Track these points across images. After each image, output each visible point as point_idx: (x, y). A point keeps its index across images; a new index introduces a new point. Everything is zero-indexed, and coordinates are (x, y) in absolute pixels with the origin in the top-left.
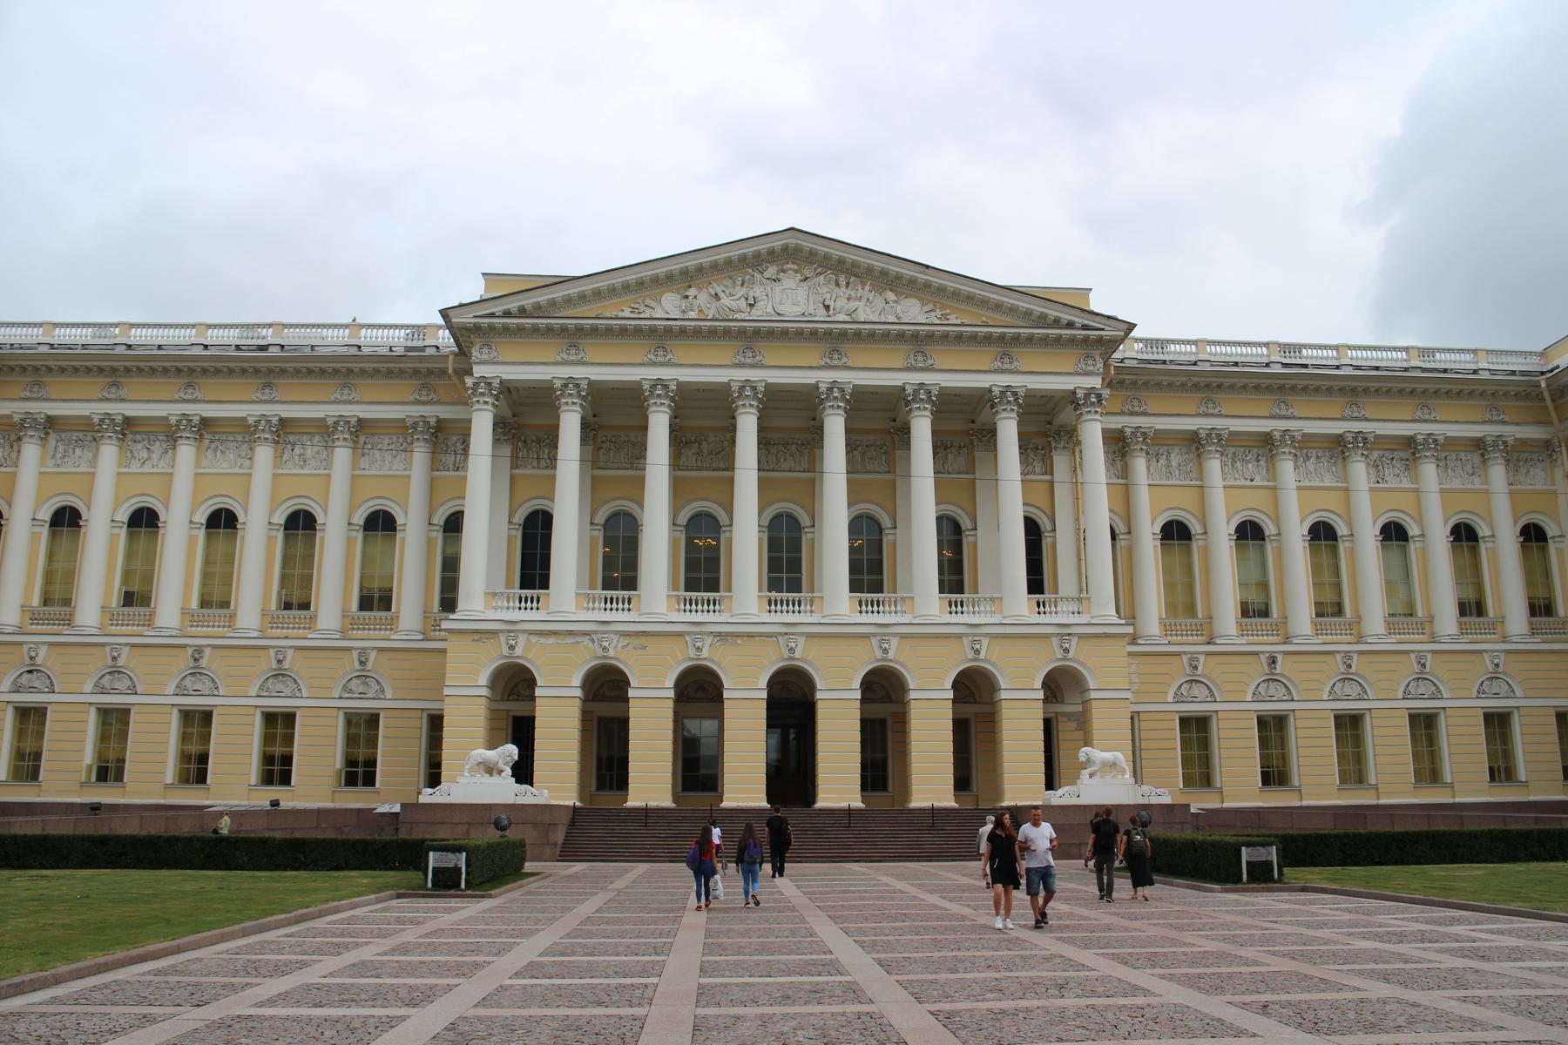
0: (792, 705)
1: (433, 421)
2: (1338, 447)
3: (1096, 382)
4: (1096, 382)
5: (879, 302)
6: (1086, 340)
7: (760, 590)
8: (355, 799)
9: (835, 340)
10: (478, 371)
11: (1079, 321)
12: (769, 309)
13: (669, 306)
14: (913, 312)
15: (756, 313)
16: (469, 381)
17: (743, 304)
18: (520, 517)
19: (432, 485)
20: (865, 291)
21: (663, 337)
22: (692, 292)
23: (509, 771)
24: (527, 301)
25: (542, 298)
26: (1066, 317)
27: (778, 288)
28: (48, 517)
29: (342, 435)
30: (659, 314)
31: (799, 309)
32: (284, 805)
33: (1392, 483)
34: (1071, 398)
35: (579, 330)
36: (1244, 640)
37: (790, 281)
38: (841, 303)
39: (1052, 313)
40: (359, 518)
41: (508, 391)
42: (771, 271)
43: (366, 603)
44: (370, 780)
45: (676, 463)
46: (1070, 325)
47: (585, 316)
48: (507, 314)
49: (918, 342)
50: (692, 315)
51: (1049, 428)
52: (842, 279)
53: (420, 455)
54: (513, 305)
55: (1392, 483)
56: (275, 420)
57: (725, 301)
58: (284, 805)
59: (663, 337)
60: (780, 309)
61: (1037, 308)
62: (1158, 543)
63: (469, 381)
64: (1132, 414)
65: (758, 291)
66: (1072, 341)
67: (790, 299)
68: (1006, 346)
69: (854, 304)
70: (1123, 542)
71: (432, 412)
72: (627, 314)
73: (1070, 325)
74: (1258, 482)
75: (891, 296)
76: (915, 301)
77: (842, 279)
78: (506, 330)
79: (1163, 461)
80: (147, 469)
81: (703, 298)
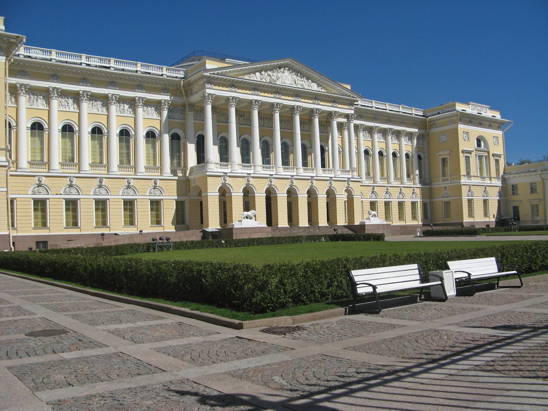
2: (384, 132)
4: (353, 112)
9: (297, 94)
15: (279, 82)
18: (196, 136)
21: (255, 87)
23: (254, 218)
28: (30, 126)
31: (290, 82)
32: (144, 232)
33: (394, 142)
34: (347, 116)
36: (382, 182)
37: (287, 73)
41: (216, 99)
42: (282, 69)
45: (238, 123)
46: (349, 96)
48: (218, 74)
49: (315, 97)
50: (264, 81)
55: (394, 142)
58: (144, 232)
59: (255, 87)
60: (286, 81)
65: (280, 75)
73: (349, 96)
74: (368, 139)
80: (67, 109)
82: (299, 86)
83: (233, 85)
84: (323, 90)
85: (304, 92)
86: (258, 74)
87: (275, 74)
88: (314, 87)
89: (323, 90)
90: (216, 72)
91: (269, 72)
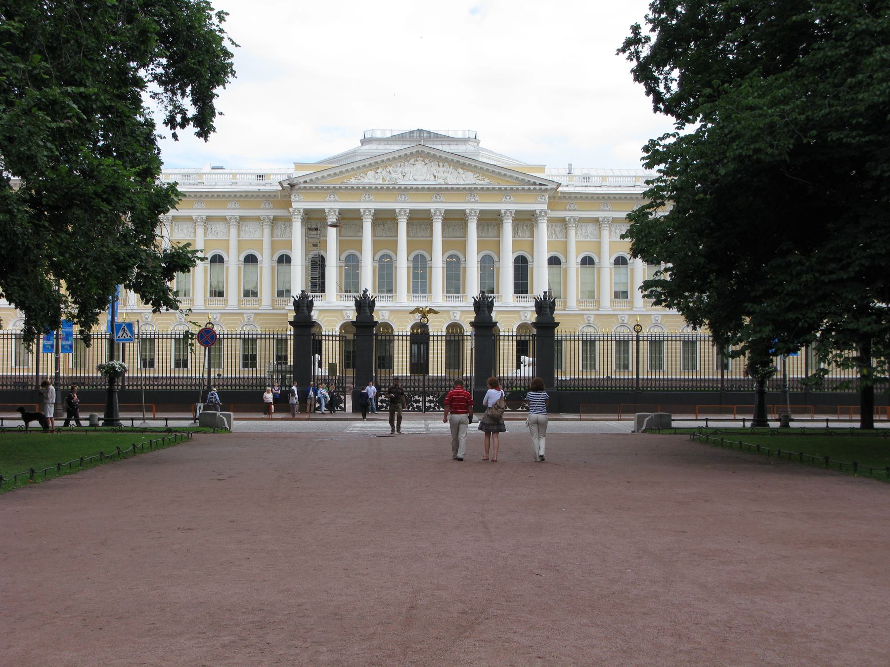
0: (420, 338)
1: (272, 218)
5: (456, 174)
6: (540, 189)
7: (408, 292)
10: (295, 205)
11: (538, 182)
12: (411, 178)
13: (371, 178)
14: (468, 179)
16: (291, 210)
17: (401, 176)
19: (273, 242)
22: (380, 170)
25: (319, 176)
26: (532, 180)
27: (414, 168)
29: (233, 224)
30: (366, 180)
35: (334, 188)
37: (420, 165)
38: (441, 174)
39: (527, 179)
40: (242, 258)
41: (307, 212)
42: (412, 161)
43: (247, 294)
44: (254, 365)
45: (374, 234)
46: (534, 183)
47: (336, 183)
50: (380, 181)
51: (526, 221)
52: (441, 164)
53: (267, 231)
54: (308, 179)
56: (204, 218)
57: (393, 175)
61: (521, 177)
62: (579, 266)
63: (291, 210)
64: (570, 210)
65: (407, 169)
66: (535, 189)
67: (419, 174)
68: (508, 192)
69: (446, 175)
70: (563, 266)
72: (353, 181)
76: (470, 173)
77: (441, 164)
78: (305, 188)
79: (584, 230)
81: (384, 173)
82: (441, 181)
84: (487, 181)
85: (447, 188)
86: (371, 174)
89: (487, 181)
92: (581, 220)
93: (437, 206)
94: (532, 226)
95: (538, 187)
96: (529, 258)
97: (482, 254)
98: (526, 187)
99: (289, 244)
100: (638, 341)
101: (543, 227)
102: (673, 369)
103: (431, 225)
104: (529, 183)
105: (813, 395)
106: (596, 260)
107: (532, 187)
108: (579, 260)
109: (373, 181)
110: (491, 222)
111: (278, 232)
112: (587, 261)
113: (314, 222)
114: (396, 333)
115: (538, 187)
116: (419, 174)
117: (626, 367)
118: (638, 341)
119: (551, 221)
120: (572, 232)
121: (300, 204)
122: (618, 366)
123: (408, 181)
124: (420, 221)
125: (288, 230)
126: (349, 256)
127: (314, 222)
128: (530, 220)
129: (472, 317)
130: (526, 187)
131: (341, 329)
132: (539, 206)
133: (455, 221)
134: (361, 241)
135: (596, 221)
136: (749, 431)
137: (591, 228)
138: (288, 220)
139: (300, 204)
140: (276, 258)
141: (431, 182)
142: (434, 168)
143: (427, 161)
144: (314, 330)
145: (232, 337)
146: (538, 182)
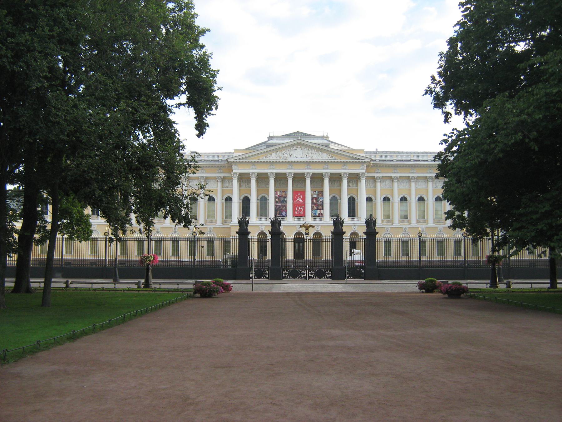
3: (364, 171)
8: (210, 258)
9: (308, 163)
10: (234, 171)
13: (273, 157)
14: (324, 157)
18: (242, 198)
20: (313, 151)
22: (278, 153)
24: (244, 156)
25: (247, 156)
26: (357, 157)
27: (296, 151)
30: (271, 158)
37: (299, 150)
38: (310, 155)
39: (355, 157)
42: (295, 148)
46: (359, 159)
47: (255, 159)
48: (240, 159)
49: (326, 163)
50: (278, 158)
51: (354, 179)
53: (219, 184)
54: (241, 157)
57: (285, 155)
59: (272, 163)
65: (292, 152)
67: (298, 155)
68: (345, 163)
69: (313, 155)
71: (222, 175)
72: (264, 158)
73: (359, 159)
75: (320, 153)
81: (280, 154)
82: (310, 158)
83: (254, 163)
84: (334, 158)
86: (273, 155)
87: (288, 152)
88: (324, 157)
90: (238, 158)
91: (283, 152)
92: (383, 178)
93: (308, 171)
94: (357, 181)
95: (361, 161)
96: (356, 198)
97: (332, 196)
98: (355, 161)
99: (231, 191)
100: (465, 241)
101: (363, 181)
102: (449, 256)
103: (304, 181)
104: (356, 159)
105: (529, 271)
106: (391, 199)
107: (357, 161)
108: (382, 199)
109: (275, 158)
110: (336, 179)
111: (225, 185)
112: (386, 199)
113: (244, 179)
114: (324, 238)
115: (361, 161)
116: (298, 155)
117: (460, 254)
118: (465, 241)
119: (368, 178)
120: (378, 184)
121: (237, 170)
122: (403, 254)
123: (293, 158)
124: (299, 179)
125: (230, 184)
126: (262, 197)
127: (244, 179)
128: (356, 178)
129: (365, 229)
130: (355, 161)
131: (313, 236)
132: (361, 171)
133: (317, 179)
134: (269, 190)
135: (391, 178)
136: (505, 290)
137: (388, 182)
138: (230, 179)
139: (237, 170)
140: (224, 198)
141: (305, 159)
142: (306, 151)
143: (303, 148)
144: (281, 236)
145: (431, 240)
146: (360, 158)
